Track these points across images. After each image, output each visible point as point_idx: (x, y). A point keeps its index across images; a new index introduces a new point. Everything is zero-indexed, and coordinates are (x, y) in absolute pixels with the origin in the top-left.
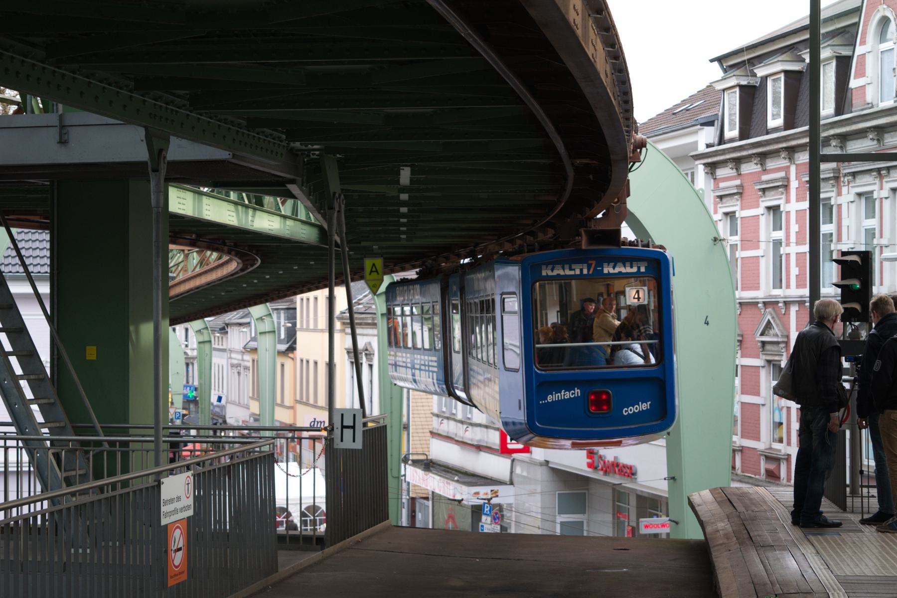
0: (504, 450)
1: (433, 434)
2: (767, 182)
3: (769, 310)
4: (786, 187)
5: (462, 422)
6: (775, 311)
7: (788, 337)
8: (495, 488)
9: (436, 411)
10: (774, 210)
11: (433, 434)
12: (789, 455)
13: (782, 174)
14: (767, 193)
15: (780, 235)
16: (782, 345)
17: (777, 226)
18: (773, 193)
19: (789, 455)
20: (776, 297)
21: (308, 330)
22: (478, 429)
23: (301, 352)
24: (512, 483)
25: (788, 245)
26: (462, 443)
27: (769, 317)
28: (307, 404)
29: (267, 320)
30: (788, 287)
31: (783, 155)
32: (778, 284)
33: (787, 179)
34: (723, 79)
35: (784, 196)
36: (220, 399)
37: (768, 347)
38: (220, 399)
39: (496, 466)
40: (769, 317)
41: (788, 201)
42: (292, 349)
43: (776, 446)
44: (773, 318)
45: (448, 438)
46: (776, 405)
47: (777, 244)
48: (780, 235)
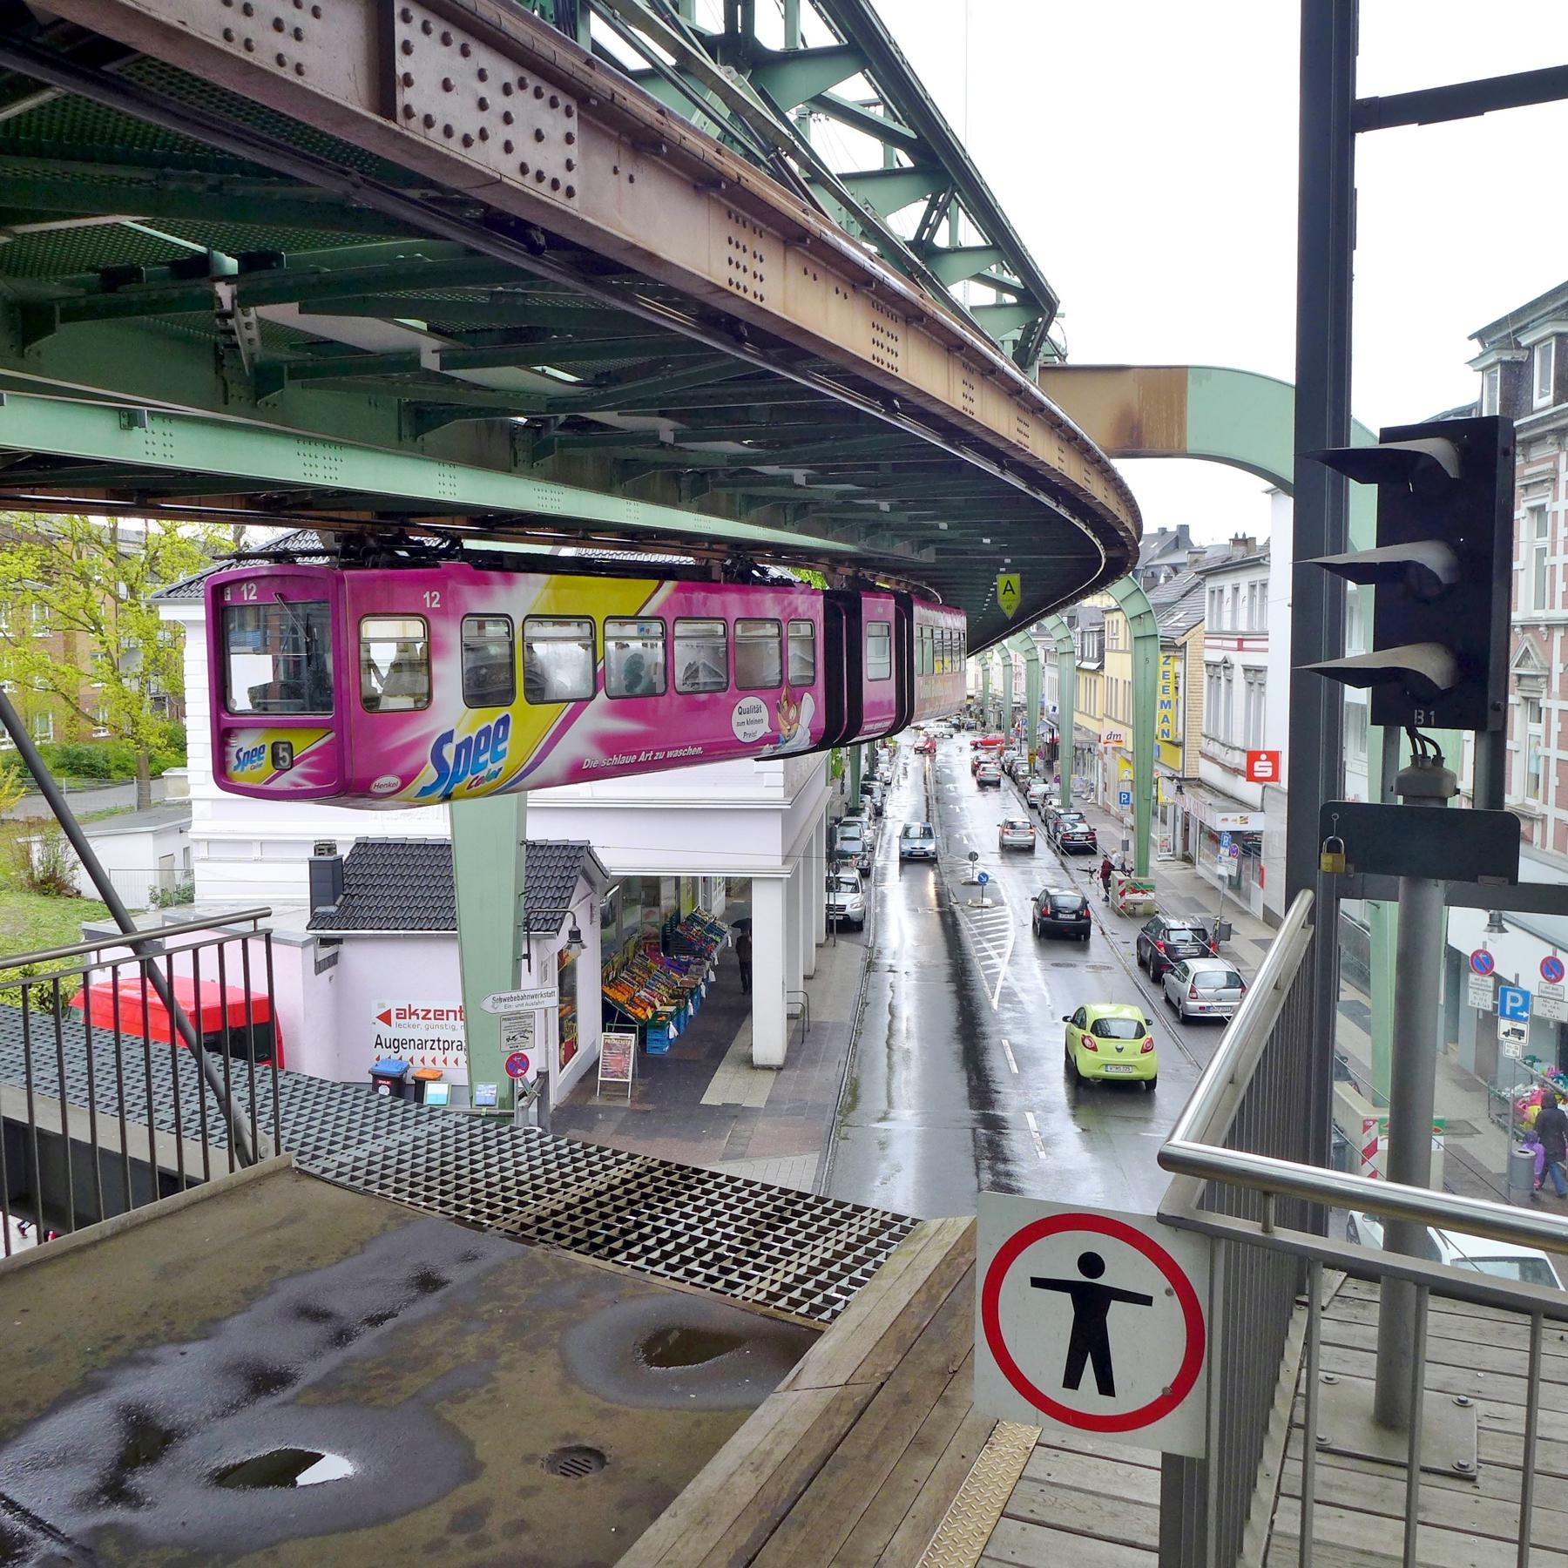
0: (1251, 777)
1: (1204, 755)
2: (1530, 476)
3: (1528, 635)
4: (1554, 481)
5: (1223, 745)
6: (1535, 637)
7: (1550, 669)
8: (1245, 815)
9: (1204, 731)
10: (1538, 511)
11: (1204, 755)
12: (1545, 816)
13: (1550, 465)
14: (1530, 490)
15: (1545, 542)
16: (1542, 680)
17: (1541, 532)
18: (1537, 490)
19: (1545, 816)
20: (1536, 619)
21: (1112, 651)
22: (1238, 752)
23: (1107, 671)
24: (1262, 811)
25: (1554, 553)
26: (1223, 766)
27: (1527, 644)
28: (1110, 718)
29: (1067, 642)
30: (1552, 607)
31: (1550, 439)
32: (1540, 604)
33: (1556, 471)
34: (1482, 355)
35: (1550, 493)
36: (1054, 709)
37: (1525, 682)
38: (1054, 709)
39: (1249, 791)
40: (1527, 644)
41: (1556, 499)
42: (1101, 667)
43: (1531, 802)
44: (1532, 645)
45: (1212, 759)
46: (1532, 752)
47: (1541, 553)
48: (1545, 542)
